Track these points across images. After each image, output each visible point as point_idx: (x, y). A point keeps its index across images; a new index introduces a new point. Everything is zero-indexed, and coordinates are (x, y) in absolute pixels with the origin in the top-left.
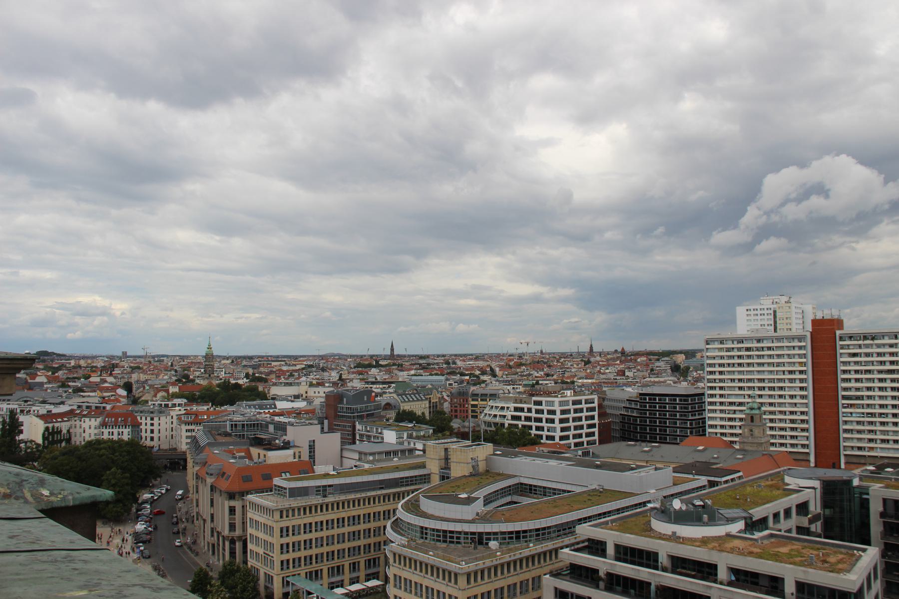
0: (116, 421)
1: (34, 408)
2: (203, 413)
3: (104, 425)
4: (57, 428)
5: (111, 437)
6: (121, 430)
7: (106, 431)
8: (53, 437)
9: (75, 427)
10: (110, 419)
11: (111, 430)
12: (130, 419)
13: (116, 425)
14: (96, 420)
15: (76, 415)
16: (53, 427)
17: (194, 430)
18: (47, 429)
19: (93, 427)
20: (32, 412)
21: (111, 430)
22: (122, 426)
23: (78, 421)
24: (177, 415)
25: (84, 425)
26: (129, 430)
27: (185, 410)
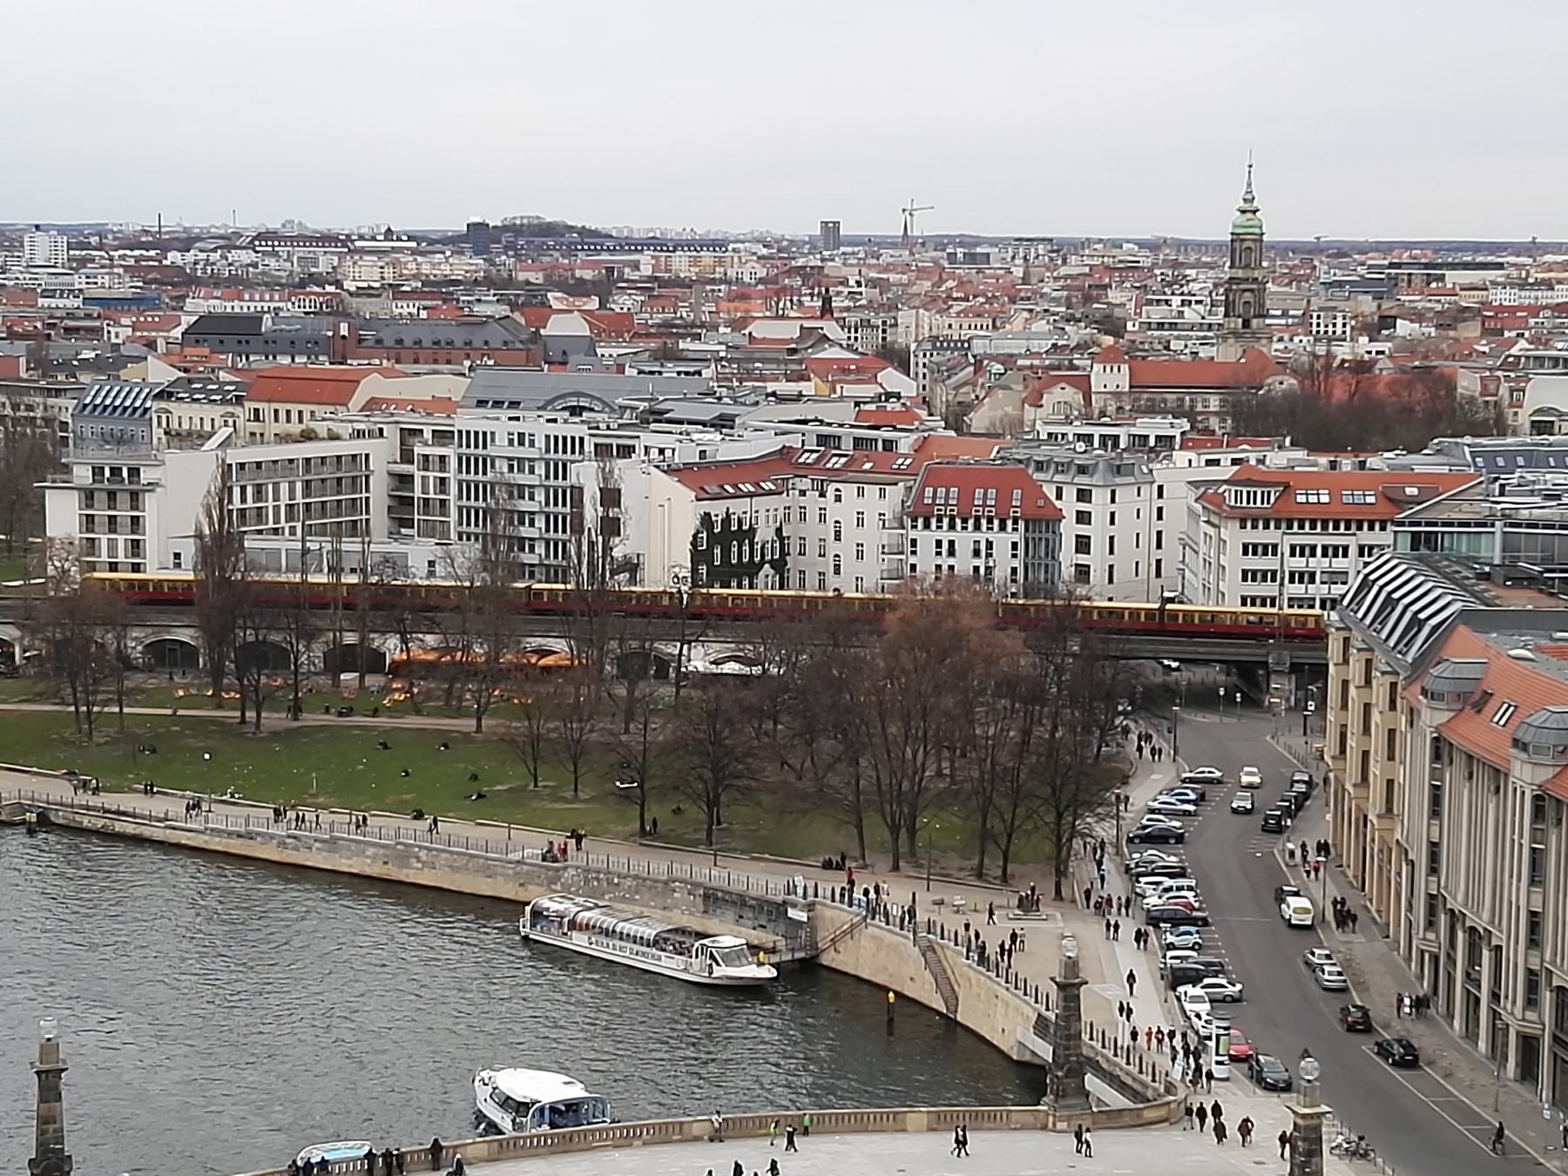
0: (966, 498)
1: (646, 438)
2: (1313, 482)
3: (919, 514)
4: (740, 521)
5: (946, 561)
6: (982, 537)
7: (926, 538)
8: (726, 554)
9: (803, 517)
10: (941, 491)
11: (945, 536)
12: (1017, 493)
13: (964, 516)
14: (882, 494)
15: (802, 470)
16: (727, 520)
17: (1275, 547)
18: (706, 519)
19: (871, 519)
20: (640, 450)
21: (945, 536)
22: (990, 521)
23: (813, 495)
24: (1195, 484)
25: (834, 511)
26: (1016, 537)
27: (1235, 462)
